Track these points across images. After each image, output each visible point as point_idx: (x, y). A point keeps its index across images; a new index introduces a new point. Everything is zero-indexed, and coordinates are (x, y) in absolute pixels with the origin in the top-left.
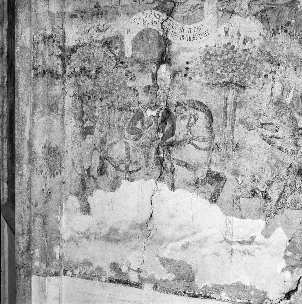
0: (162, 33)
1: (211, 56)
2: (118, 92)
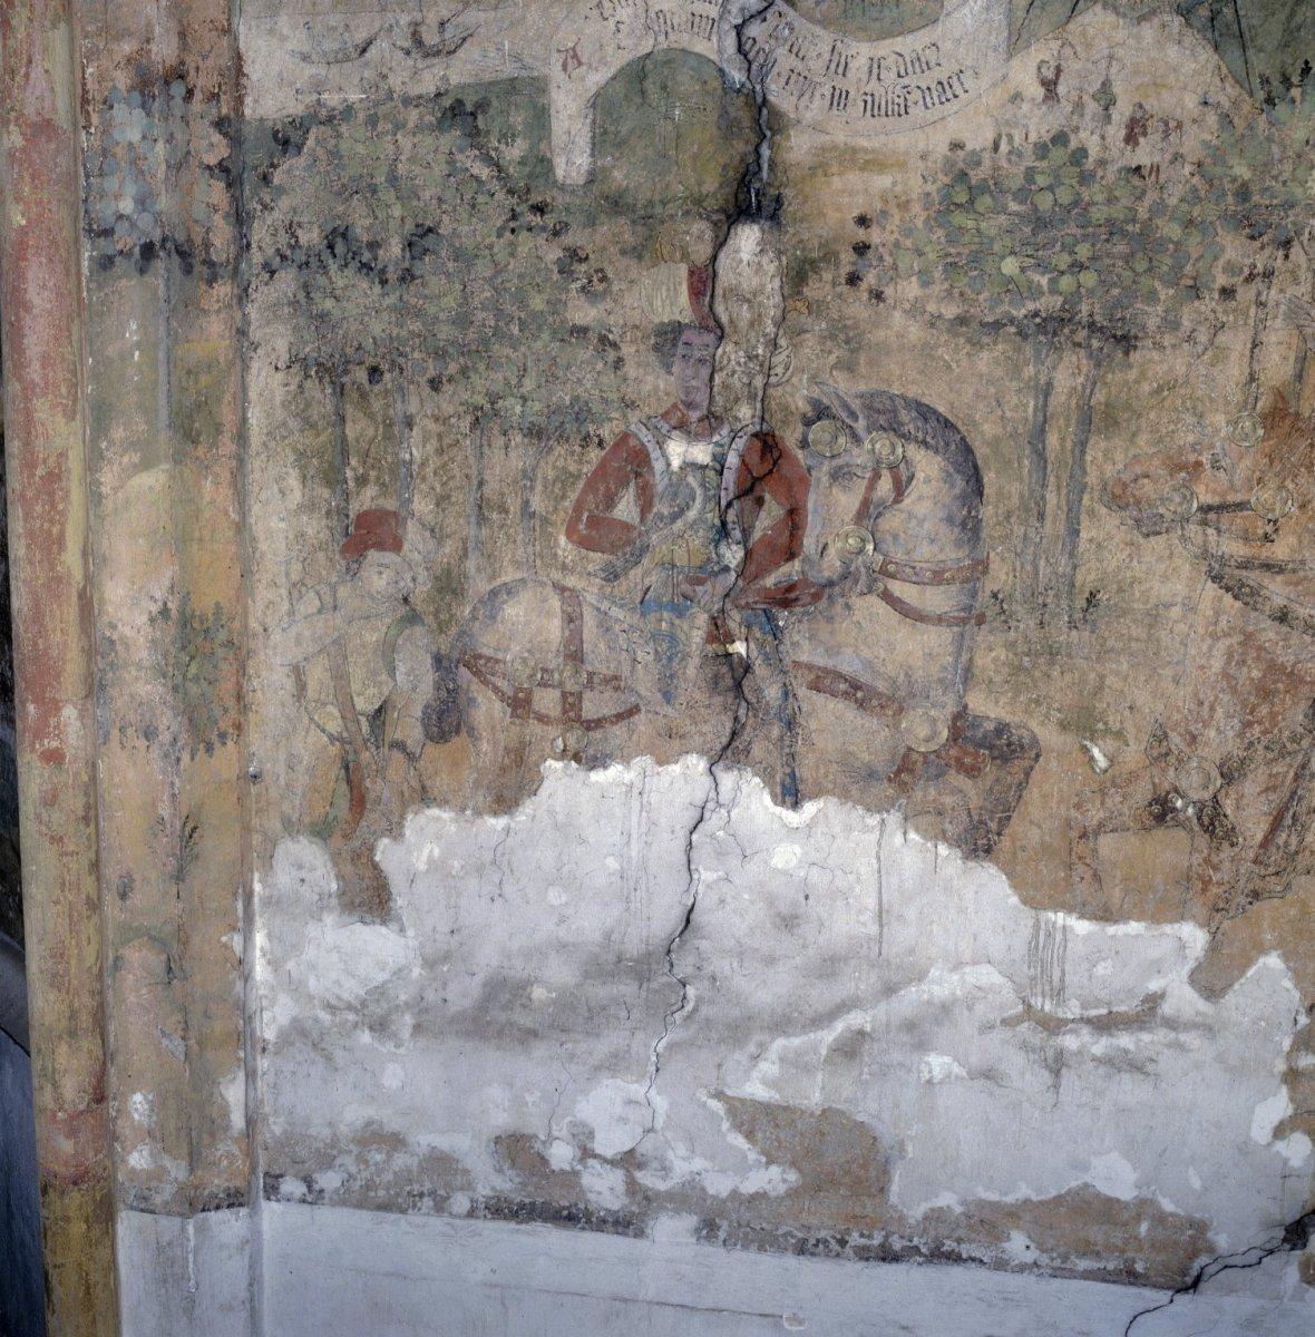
0: (737, 76)
1: (975, 192)
2: (523, 349)
